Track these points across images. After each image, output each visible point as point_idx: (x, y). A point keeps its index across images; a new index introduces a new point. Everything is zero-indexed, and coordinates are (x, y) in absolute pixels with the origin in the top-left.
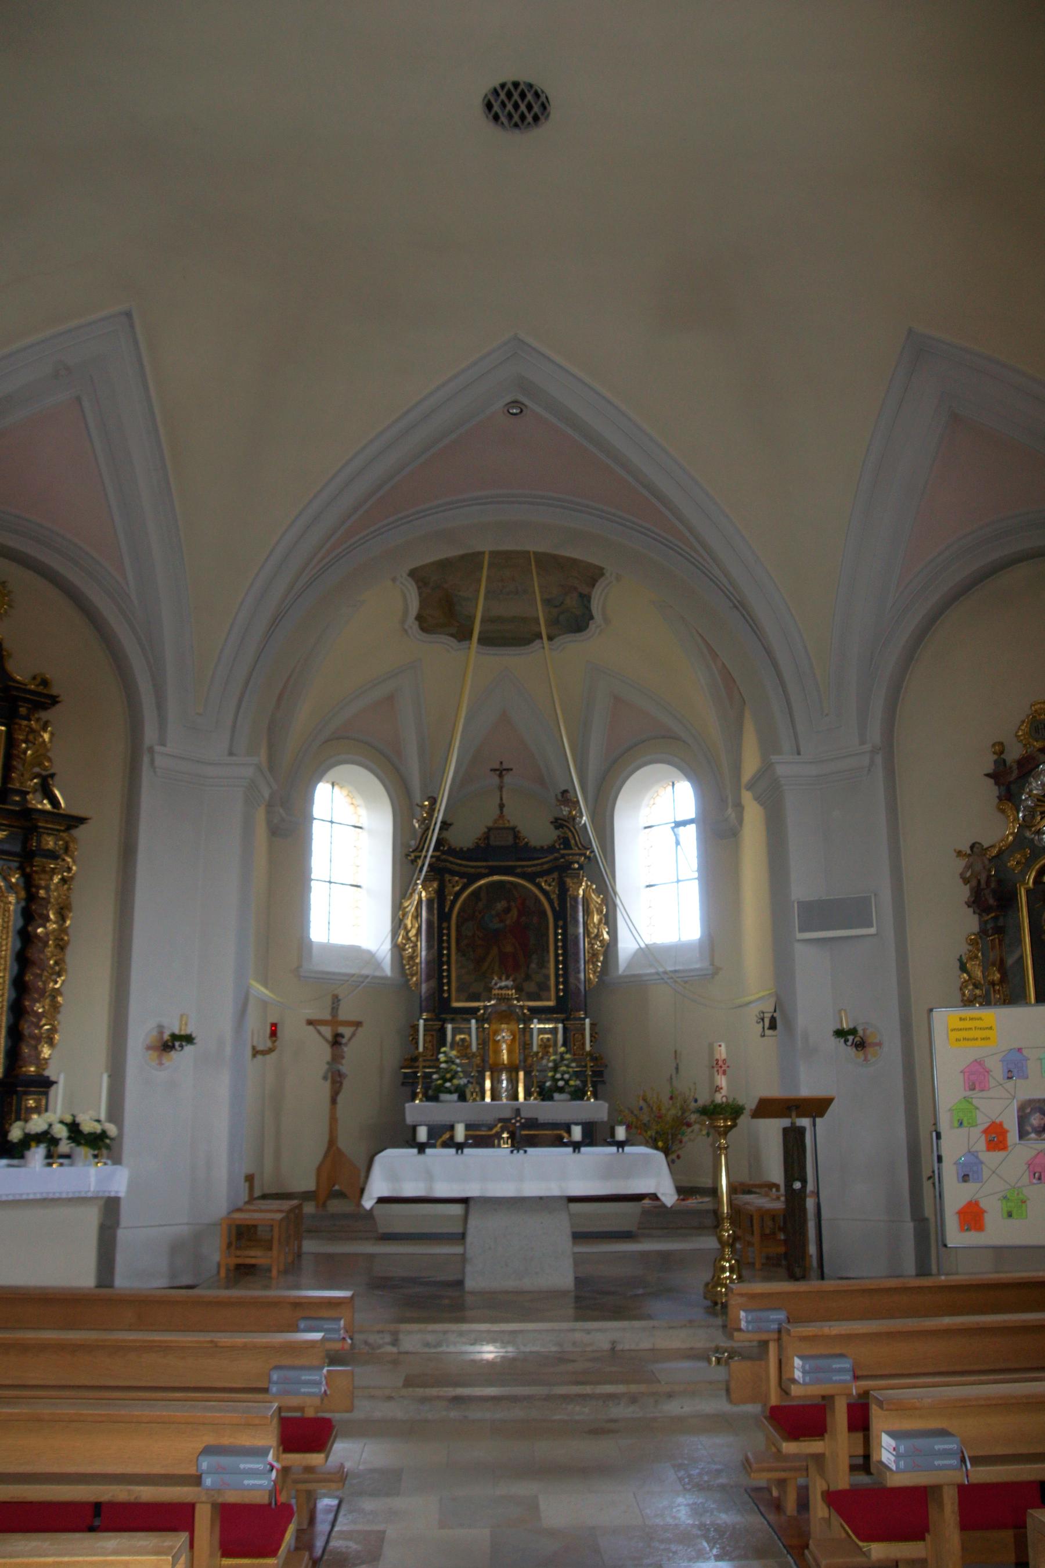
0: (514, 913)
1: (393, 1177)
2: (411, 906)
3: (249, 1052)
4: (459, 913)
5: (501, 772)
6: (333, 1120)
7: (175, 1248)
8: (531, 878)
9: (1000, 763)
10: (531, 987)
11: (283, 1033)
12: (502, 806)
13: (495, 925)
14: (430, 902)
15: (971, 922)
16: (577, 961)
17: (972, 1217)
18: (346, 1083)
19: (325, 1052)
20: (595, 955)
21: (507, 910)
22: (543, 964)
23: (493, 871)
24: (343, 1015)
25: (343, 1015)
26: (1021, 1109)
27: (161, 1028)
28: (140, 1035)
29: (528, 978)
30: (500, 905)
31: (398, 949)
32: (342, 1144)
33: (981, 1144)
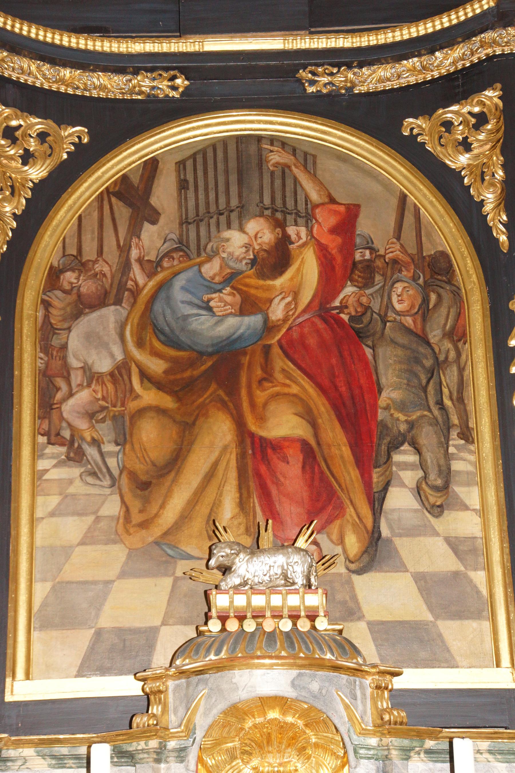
0: (307, 270)
4: (54, 275)
8: (377, 116)
13: (221, 323)
23: (214, 85)
29: (374, 552)
30: (243, 239)
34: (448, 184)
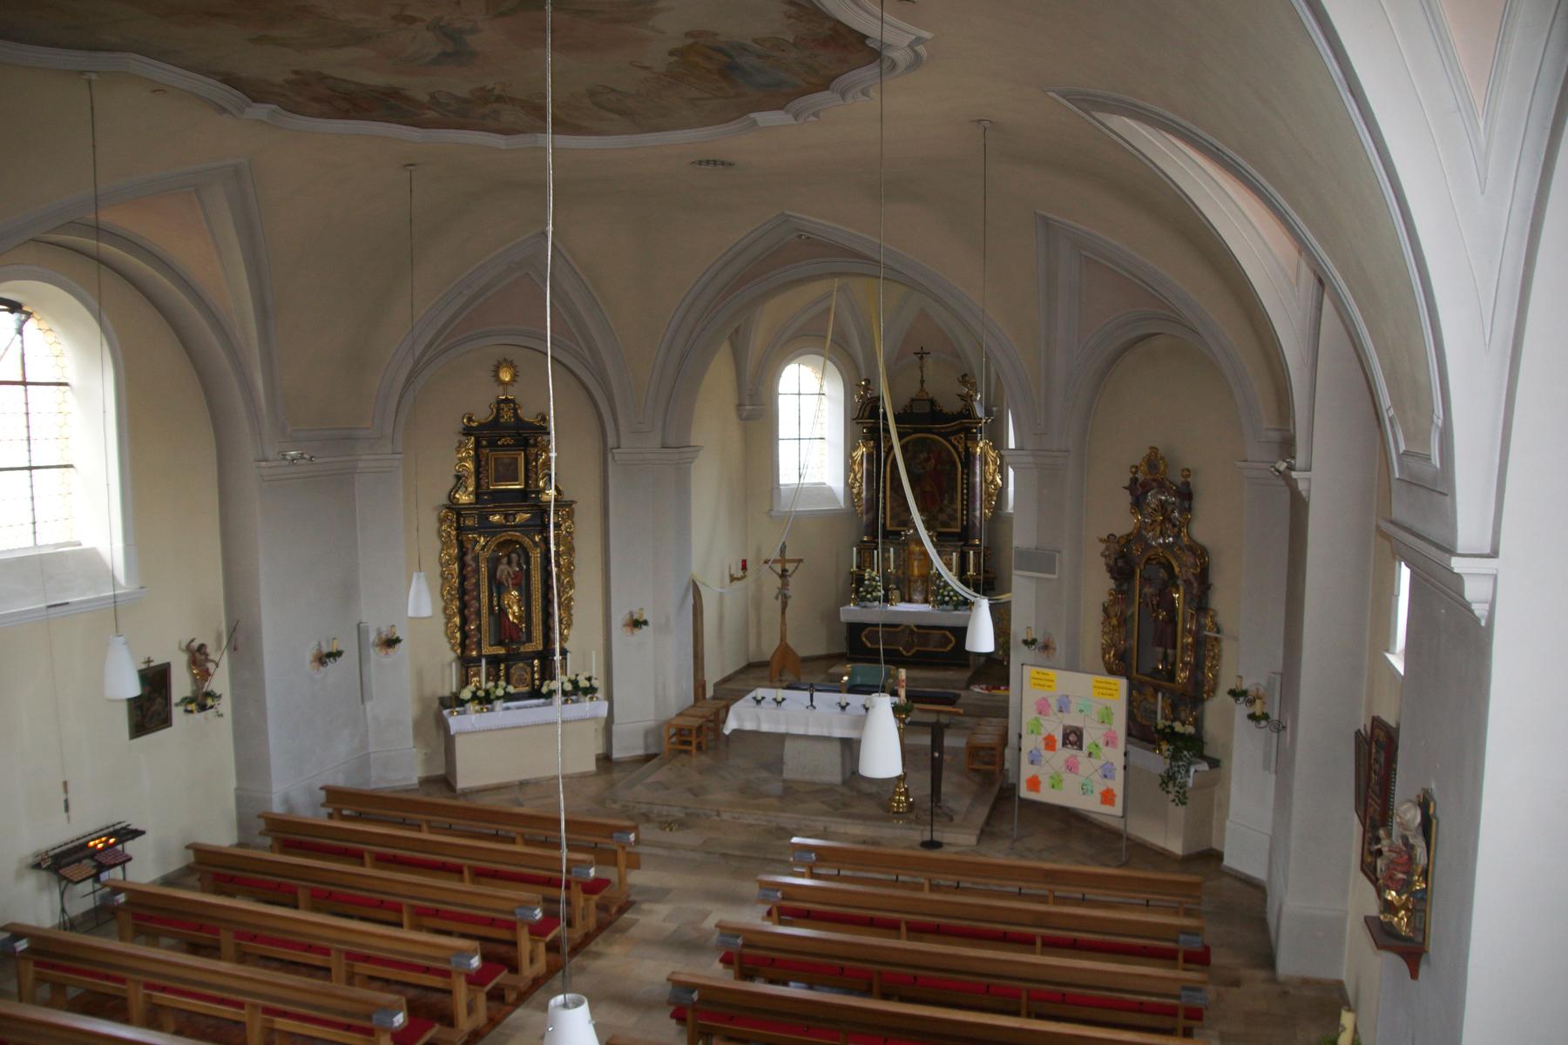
1: (739, 718)
2: (858, 454)
3: (727, 579)
5: (922, 355)
6: (783, 623)
7: (647, 734)
8: (946, 436)
9: (1134, 481)
10: (942, 517)
11: (749, 565)
12: (922, 382)
14: (870, 455)
15: (1112, 584)
16: (974, 503)
17: (1034, 784)
18: (790, 602)
19: (778, 582)
20: (990, 495)
21: (928, 460)
22: (952, 501)
23: (916, 431)
24: (788, 557)
25: (788, 557)
26: (1065, 728)
27: (631, 614)
28: (619, 618)
29: (941, 510)
31: (849, 486)
32: (791, 642)
33: (1042, 746)
34: (956, 448)
